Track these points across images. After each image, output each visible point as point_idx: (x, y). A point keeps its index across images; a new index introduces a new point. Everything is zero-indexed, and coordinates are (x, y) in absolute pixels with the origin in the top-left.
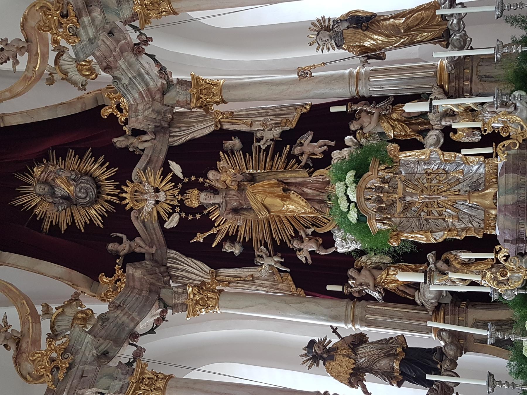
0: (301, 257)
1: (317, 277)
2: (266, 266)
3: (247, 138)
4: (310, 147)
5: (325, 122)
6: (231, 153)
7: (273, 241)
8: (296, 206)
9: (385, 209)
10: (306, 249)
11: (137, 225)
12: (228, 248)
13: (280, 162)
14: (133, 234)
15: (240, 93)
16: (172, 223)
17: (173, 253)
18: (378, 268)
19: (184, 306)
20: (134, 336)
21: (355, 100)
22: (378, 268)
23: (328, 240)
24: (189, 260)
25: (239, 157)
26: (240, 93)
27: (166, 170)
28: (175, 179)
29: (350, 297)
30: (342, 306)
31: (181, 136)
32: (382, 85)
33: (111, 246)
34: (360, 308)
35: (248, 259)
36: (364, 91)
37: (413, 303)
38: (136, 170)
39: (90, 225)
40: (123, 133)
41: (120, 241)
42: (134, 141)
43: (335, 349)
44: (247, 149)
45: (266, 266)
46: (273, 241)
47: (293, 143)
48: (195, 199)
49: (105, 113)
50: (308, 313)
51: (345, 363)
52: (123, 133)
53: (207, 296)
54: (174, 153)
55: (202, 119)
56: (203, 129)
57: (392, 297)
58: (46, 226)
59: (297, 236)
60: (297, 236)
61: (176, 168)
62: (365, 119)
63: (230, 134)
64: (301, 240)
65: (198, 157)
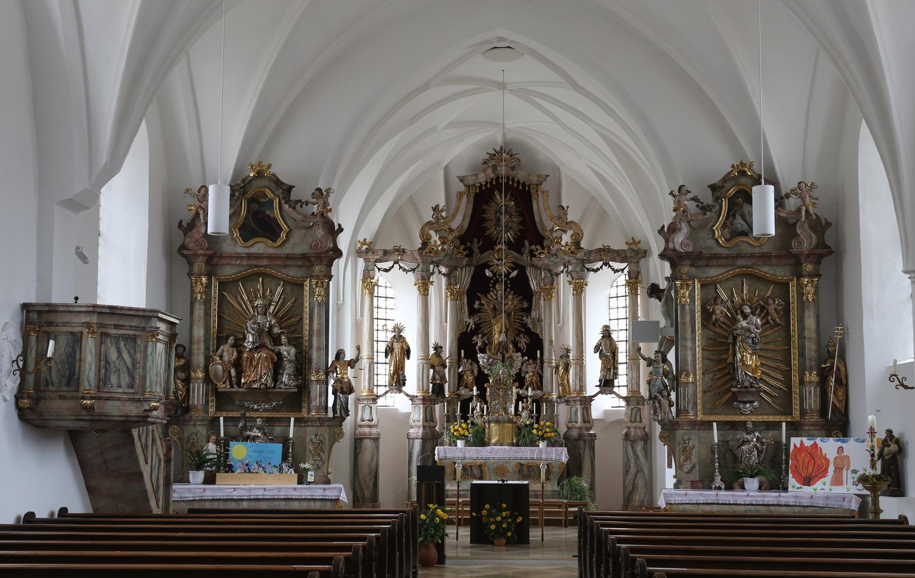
0: (475, 338)
1: (466, 343)
2: (469, 321)
3: (528, 311)
4: (523, 341)
5: (533, 346)
6: (521, 301)
7: (481, 324)
8: (498, 337)
9: (498, 382)
10: (478, 341)
11: (487, 253)
12: (477, 303)
13: (517, 326)
14: (482, 250)
15: (547, 309)
16: (488, 273)
17: (473, 268)
18: (472, 372)
19: (449, 284)
20: (438, 266)
21: (542, 362)
22: (472, 372)
23: (483, 351)
24: (470, 279)
25: (519, 306)
26: (547, 306)
27: (513, 269)
28: (509, 273)
29: (459, 360)
30: (455, 357)
31: (530, 273)
32: (547, 372)
33: (476, 240)
34: (455, 364)
35: (472, 312)
36: (545, 365)
37: (459, 386)
38: (514, 253)
39: (485, 229)
40: (531, 245)
41: (478, 243)
42: (527, 251)
43: (440, 357)
44: (522, 310)
45: (469, 321)
46: (481, 324)
47: (525, 333)
48: (500, 288)
49: (538, 247)
50: (451, 343)
51: (436, 361)
52: (531, 245)
53: (455, 297)
54: (522, 270)
55: (538, 284)
56: (533, 285)
57: (460, 376)
58: (485, 207)
59: (484, 335)
60: (484, 335)
61: (514, 274)
62: (533, 366)
63: (530, 302)
64: (482, 338)
65: (520, 287)
